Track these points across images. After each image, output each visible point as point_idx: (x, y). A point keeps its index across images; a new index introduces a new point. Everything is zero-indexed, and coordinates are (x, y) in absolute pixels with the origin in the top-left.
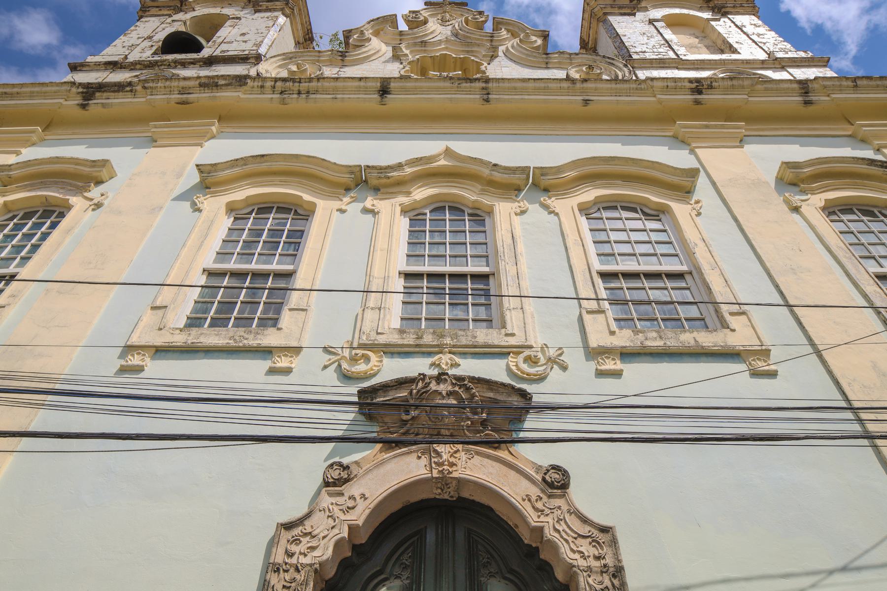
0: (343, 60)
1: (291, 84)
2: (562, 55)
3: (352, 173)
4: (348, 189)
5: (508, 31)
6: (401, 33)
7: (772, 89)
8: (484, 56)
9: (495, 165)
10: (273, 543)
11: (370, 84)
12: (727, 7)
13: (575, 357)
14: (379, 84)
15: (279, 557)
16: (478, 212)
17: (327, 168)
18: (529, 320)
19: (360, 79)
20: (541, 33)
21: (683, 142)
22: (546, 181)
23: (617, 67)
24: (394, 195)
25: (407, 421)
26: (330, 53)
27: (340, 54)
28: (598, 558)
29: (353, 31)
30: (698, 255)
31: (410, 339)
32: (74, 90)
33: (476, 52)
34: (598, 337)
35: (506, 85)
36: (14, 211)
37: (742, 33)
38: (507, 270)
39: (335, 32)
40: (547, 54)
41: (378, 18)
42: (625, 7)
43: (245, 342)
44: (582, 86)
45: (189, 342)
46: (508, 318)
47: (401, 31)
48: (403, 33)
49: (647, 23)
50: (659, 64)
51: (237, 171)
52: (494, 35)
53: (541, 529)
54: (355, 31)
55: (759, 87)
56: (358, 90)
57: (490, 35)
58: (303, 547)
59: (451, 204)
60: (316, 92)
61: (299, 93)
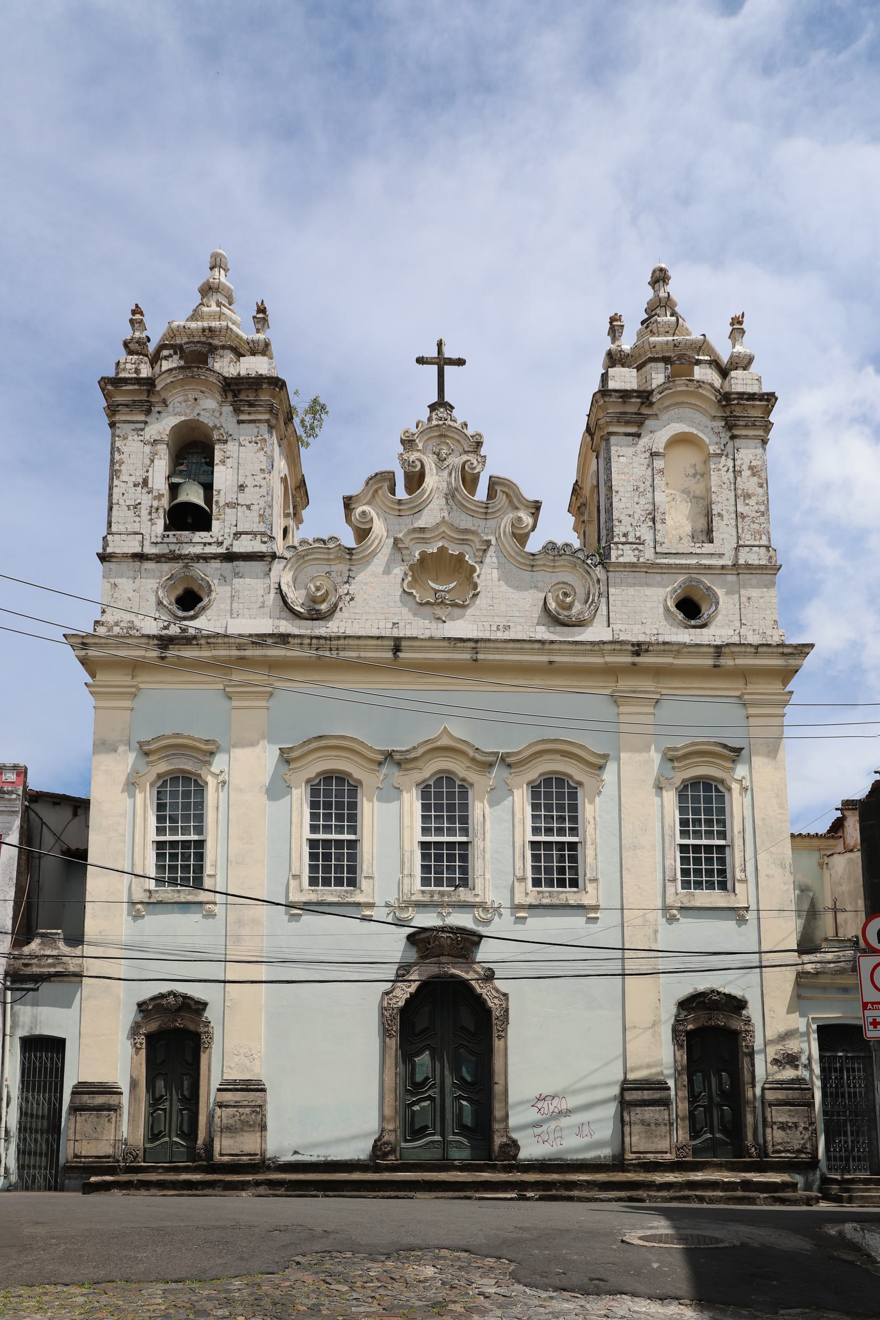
0: (350, 559)
1: (324, 642)
2: (547, 556)
3: (382, 754)
4: (380, 764)
5: (503, 492)
6: (400, 502)
7: (693, 653)
8: (478, 550)
9: (477, 749)
10: (382, 999)
11: (386, 643)
12: (739, 425)
13: (506, 913)
14: (392, 643)
15: (386, 1005)
16: (464, 784)
17: (365, 748)
18: (487, 886)
19: (378, 638)
20: (534, 504)
21: (615, 702)
22: (509, 760)
23: (592, 579)
24: (411, 772)
25: (429, 949)
26: (338, 548)
27: (348, 552)
28: (500, 1005)
29: (353, 499)
30: (587, 833)
31: (427, 898)
32: (151, 642)
33: (471, 540)
34: (519, 899)
35: (491, 645)
36: (163, 777)
37: (732, 487)
38: (478, 843)
39: (314, 398)
40: (533, 555)
41: (376, 475)
42: (632, 422)
43: (347, 899)
44: (549, 647)
45: (320, 899)
46: (476, 883)
47: (400, 500)
48: (402, 502)
49: (648, 454)
50: (632, 567)
51: (306, 749)
52: (489, 505)
53: (481, 994)
54: (356, 498)
55: (685, 650)
56: (377, 648)
57: (484, 505)
58: (394, 1001)
59: (447, 775)
60: (344, 649)
61: (331, 650)
